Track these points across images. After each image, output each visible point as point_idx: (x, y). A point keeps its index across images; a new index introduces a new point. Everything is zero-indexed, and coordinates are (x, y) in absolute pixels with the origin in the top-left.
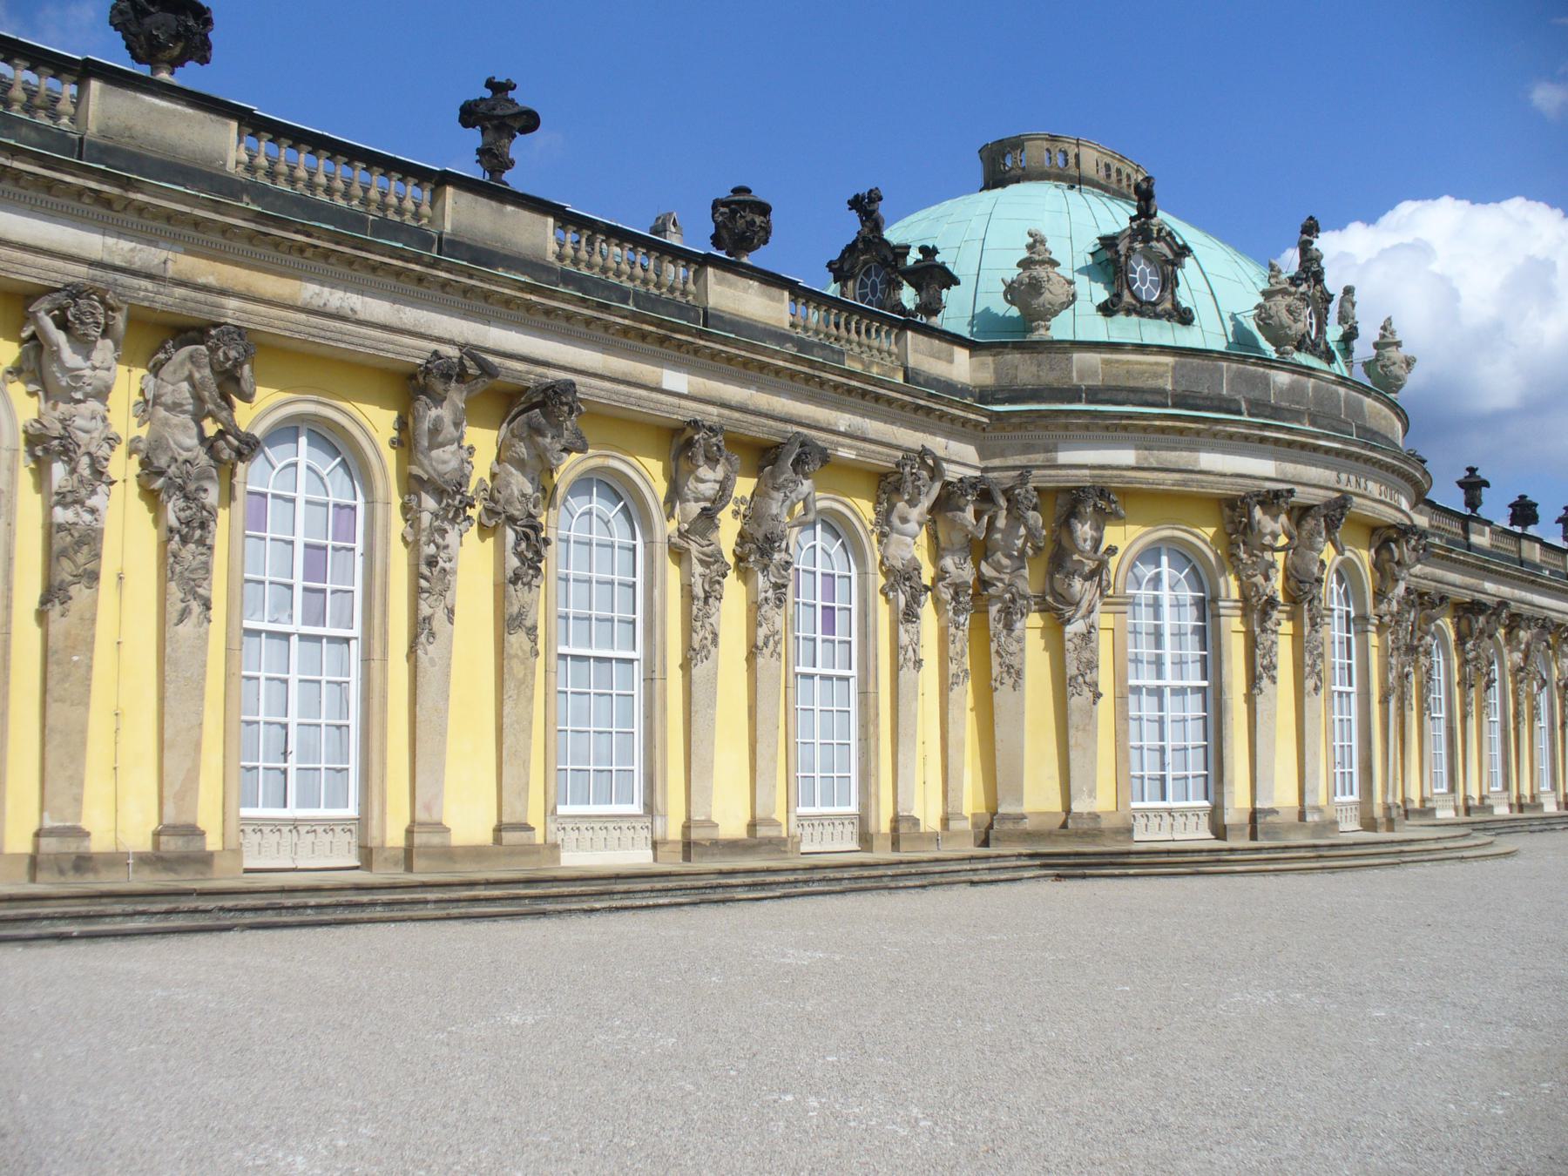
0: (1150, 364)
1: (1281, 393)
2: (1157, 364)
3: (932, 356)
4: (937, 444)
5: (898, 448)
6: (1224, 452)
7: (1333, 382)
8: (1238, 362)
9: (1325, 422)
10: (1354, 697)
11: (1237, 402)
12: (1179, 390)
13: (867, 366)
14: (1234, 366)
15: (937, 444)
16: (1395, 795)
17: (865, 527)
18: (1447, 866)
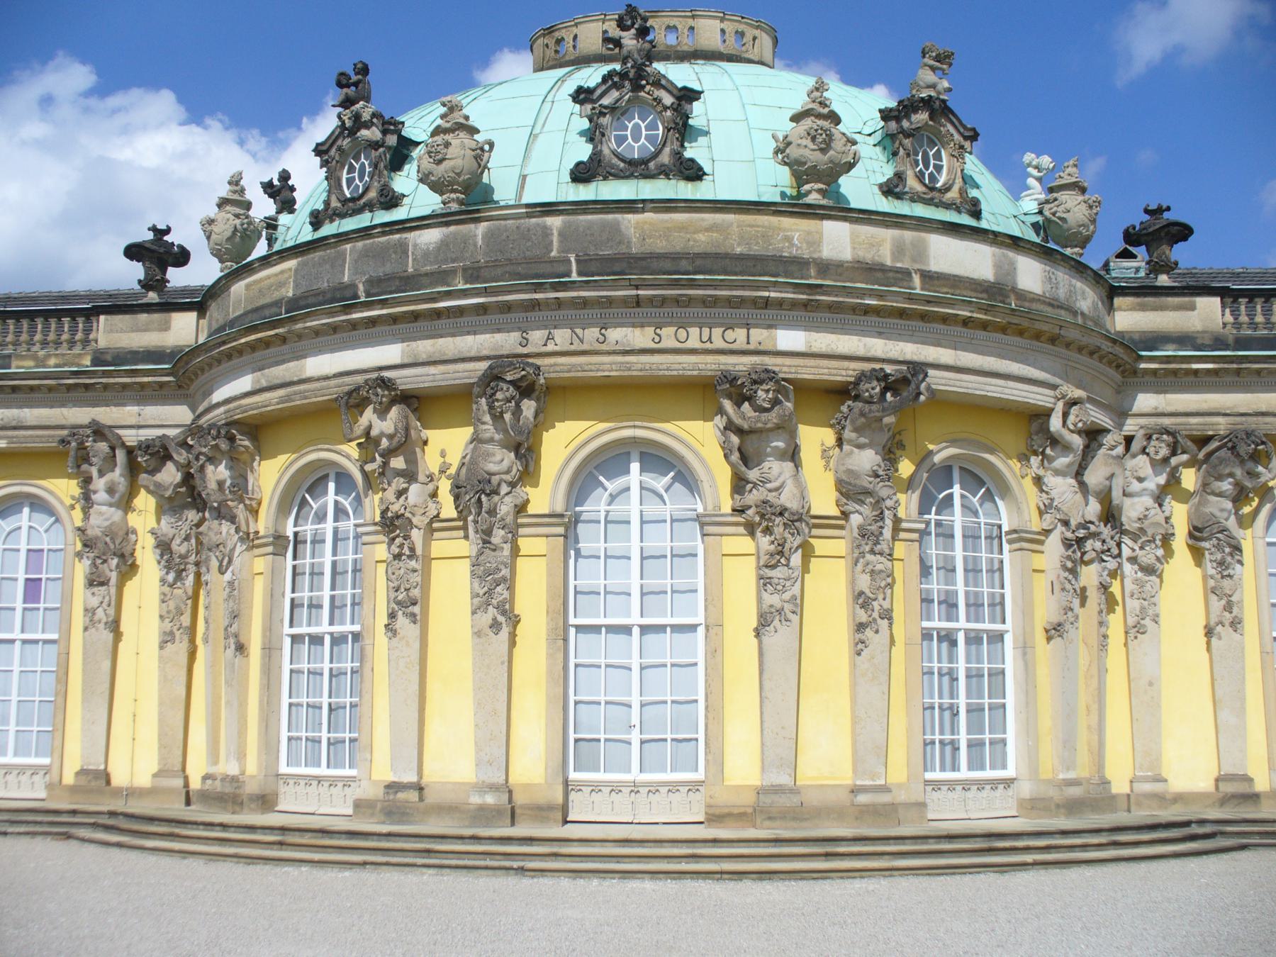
0: (276, 275)
1: (426, 254)
2: (282, 272)
3: (138, 330)
4: (106, 415)
5: (62, 427)
6: (333, 351)
7: (529, 215)
8: (362, 238)
9: (499, 271)
10: (1008, 639)
11: (353, 286)
12: (298, 293)
13: (41, 362)
14: (360, 244)
15: (106, 415)
16: (241, 756)
17: (62, 503)
18: (633, 884)
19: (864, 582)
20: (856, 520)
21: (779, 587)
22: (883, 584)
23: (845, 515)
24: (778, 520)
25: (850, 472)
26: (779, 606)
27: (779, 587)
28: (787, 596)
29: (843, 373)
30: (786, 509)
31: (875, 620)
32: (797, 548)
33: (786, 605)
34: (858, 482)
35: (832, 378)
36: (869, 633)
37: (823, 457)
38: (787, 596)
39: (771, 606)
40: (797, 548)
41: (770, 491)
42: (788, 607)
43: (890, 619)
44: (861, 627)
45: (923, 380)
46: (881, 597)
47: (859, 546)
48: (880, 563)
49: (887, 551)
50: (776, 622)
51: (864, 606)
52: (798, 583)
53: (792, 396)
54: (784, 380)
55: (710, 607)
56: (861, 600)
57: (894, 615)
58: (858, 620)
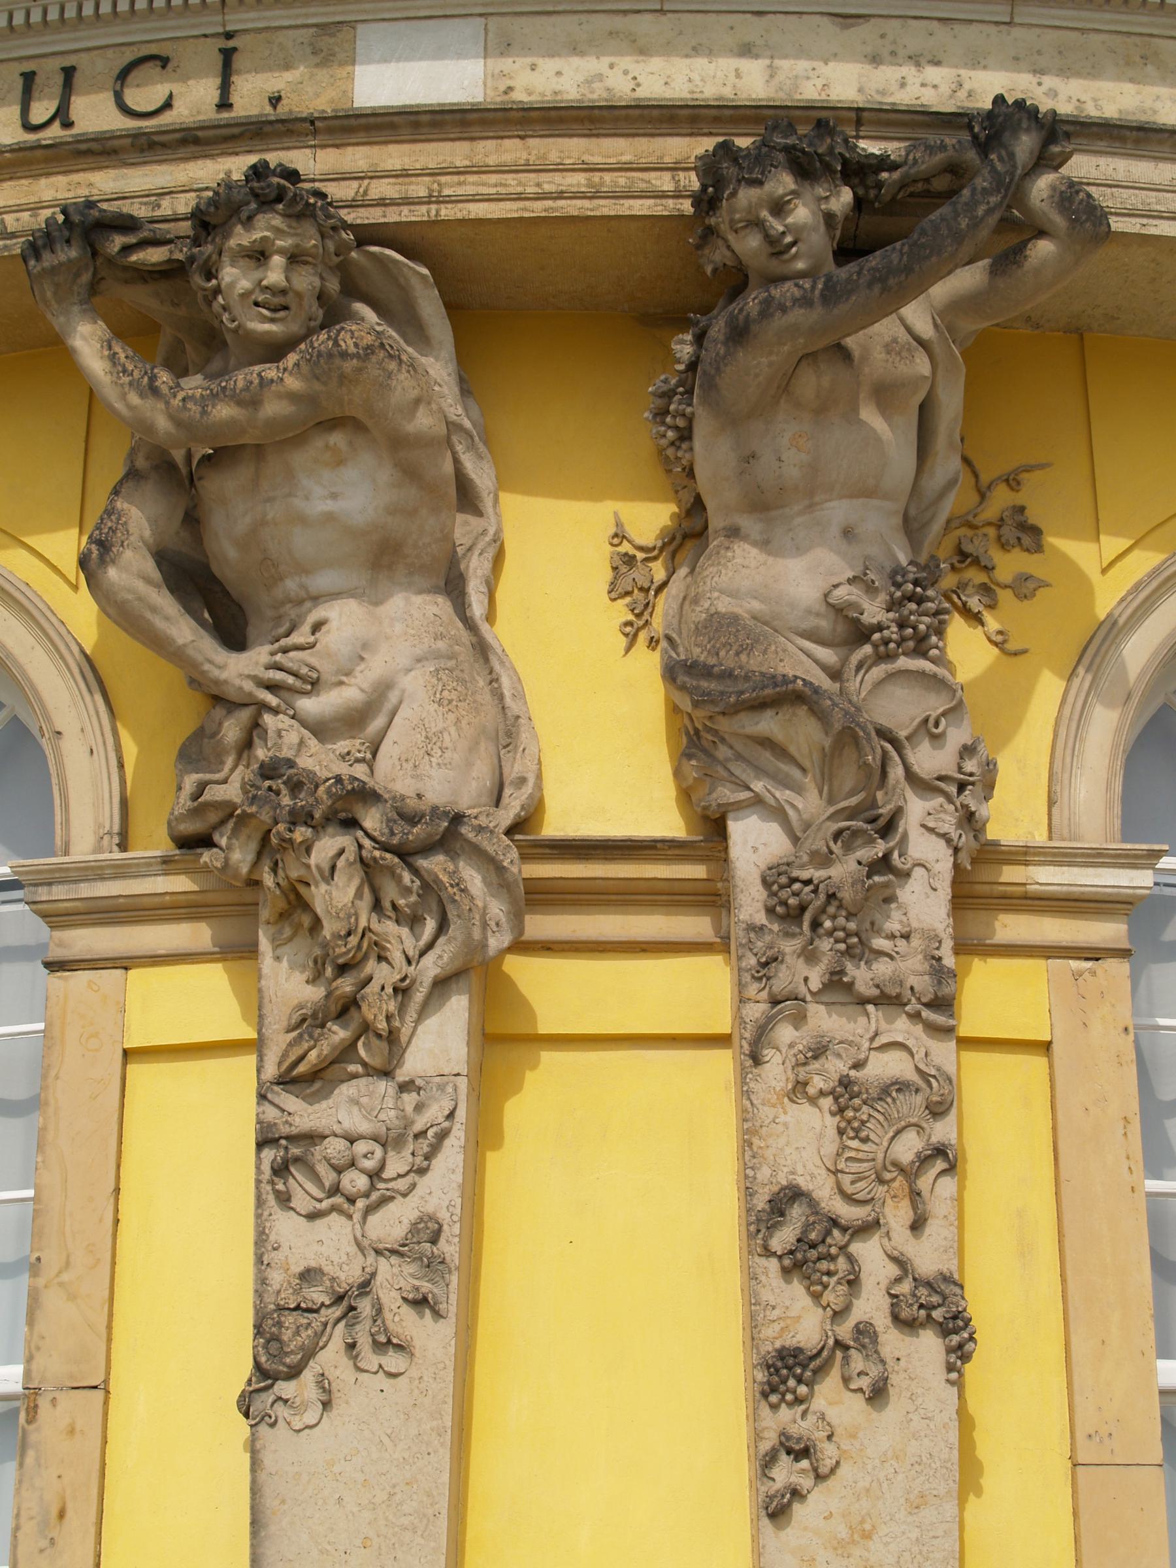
19: (804, 1145)
20: (755, 843)
21: (355, 1181)
22: (908, 1148)
23: (715, 828)
24: (328, 845)
25: (720, 626)
26: (350, 1274)
27: (355, 1181)
28: (391, 1223)
29: (656, 179)
30: (367, 795)
31: (865, 1334)
32: (443, 985)
33: (386, 1269)
34: (754, 662)
35: (607, 208)
36: (834, 1402)
37: (615, 592)
38: (391, 1223)
39: (308, 1275)
40: (443, 985)
41: (321, 730)
42: (395, 1280)
43: (956, 1332)
44: (785, 1373)
45: (1044, 161)
46: (897, 1216)
47: (769, 962)
48: (891, 1051)
49: (923, 983)
50: (331, 1357)
51: (801, 1263)
52: (451, 1157)
53: (430, 307)
54: (366, 236)
55: (53, 1300)
56: (797, 1236)
57: (983, 1303)
58: (774, 1337)
